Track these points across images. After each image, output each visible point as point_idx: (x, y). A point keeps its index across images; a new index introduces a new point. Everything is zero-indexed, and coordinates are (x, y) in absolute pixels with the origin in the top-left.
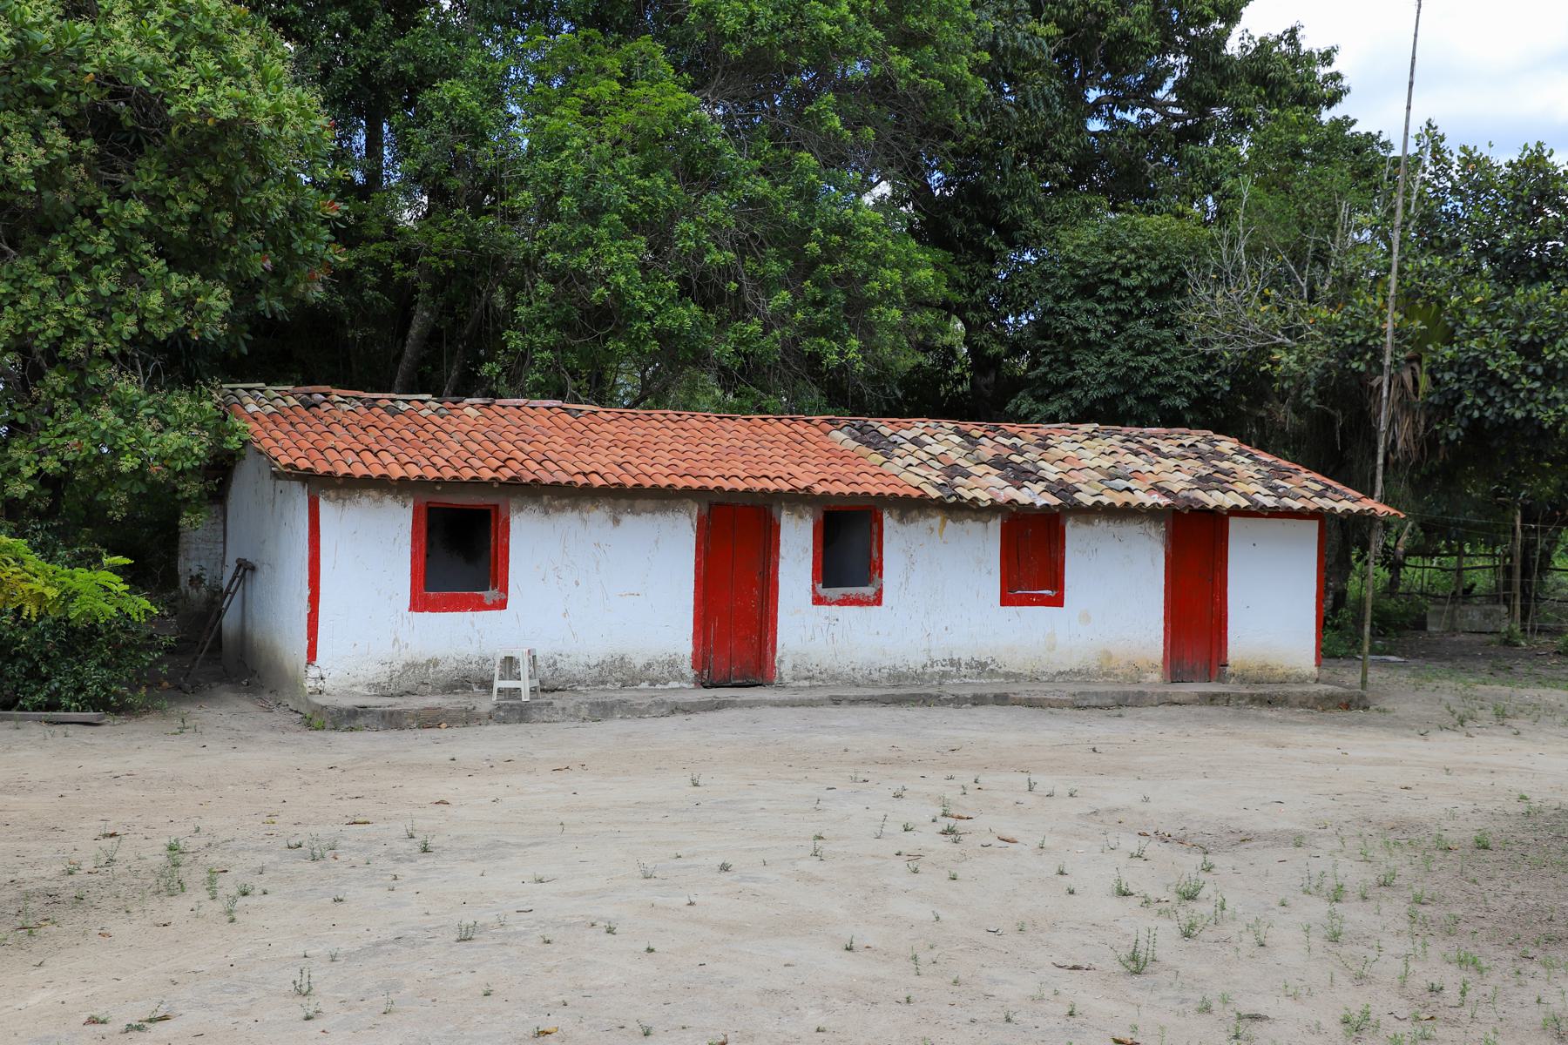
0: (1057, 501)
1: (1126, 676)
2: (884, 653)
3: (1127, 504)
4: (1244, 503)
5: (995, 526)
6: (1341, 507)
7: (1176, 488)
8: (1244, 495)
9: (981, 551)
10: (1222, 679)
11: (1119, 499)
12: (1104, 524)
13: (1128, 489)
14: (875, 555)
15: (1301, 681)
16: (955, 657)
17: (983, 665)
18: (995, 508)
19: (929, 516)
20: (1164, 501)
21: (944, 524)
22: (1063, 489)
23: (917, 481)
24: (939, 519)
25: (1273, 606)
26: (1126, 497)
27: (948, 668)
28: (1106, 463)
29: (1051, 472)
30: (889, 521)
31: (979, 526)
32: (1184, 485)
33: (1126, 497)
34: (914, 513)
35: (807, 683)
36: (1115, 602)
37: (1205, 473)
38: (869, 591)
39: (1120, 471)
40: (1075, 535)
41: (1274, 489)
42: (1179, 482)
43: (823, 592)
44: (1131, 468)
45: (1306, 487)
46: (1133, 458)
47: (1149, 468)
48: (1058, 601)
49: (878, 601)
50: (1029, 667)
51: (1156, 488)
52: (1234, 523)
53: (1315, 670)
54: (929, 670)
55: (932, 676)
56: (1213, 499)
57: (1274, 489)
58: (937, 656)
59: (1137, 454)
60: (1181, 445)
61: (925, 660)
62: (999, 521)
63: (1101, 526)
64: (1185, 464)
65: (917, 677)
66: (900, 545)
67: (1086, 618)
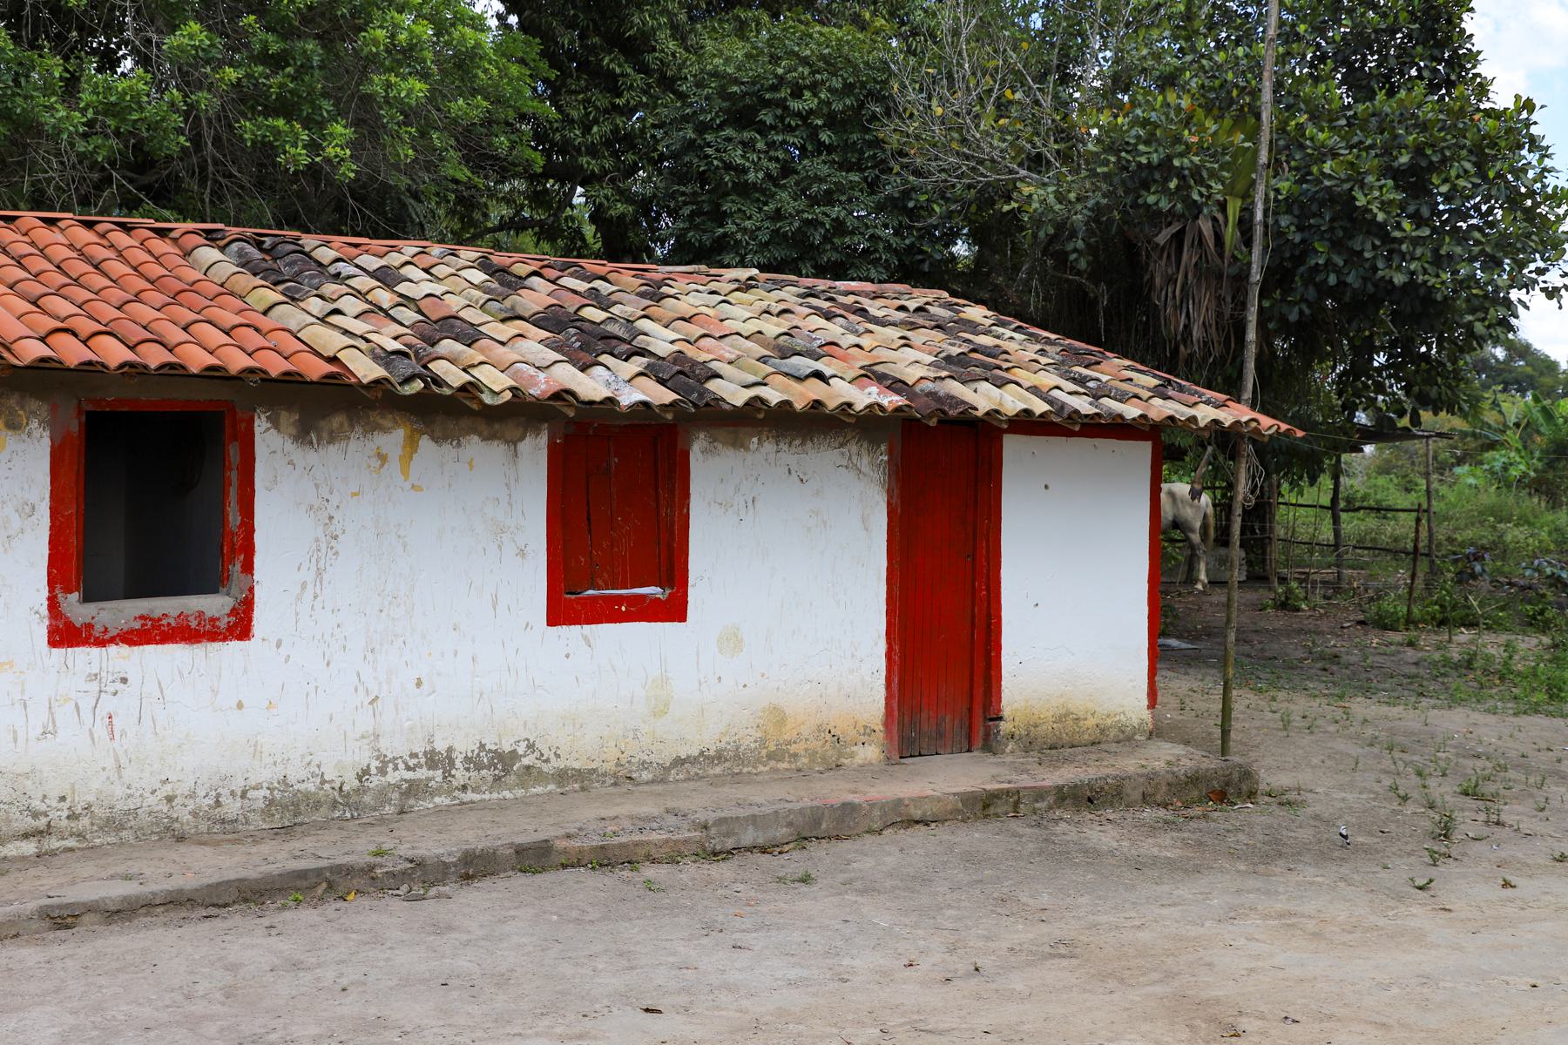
0: (668, 396)
1: (812, 755)
2: (257, 751)
3: (817, 403)
4: (1039, 407)
5: (534, 453)
6: (1205, 414)
7: (911, 375)
8: (1034, 390)
9: (499, 515)
10: (990, 745)
11: (802, 395)
12: (769, 446)
13: (818, 375)
14: (234, 518)
15: (1126, 738)
16: (441, 746)
17: (501, 763)
18: (521, 413)
19: (376, 427)
20: (891, 400)
21: (412, 445)
22: (682, 373)
23: (330, 341)
24: (399, 434)
25: (1075, 607)
26: (814, 390)
27: (423, 773)
28: (772, 327)
29: (661, 340)
30: (271, 445)
31: (497, 450)
32: (920, 372)
33: (814, 390)
34: (337, 420)
35: (29, 848)
36: (786, 605)
37: (955, 351)
38: (215, 605)
39: (799, 343)
40: (713, 476)
41: (1081, 381)
42: (914, 363)
43: (77, 609)
44: (823, 337)
45: (1133, 389)
46: (822, 322)
47: (852, 339)
48: (675, 610)
49: (240, 626)
50: (612, 754)
51: (871, 374)
52: (1012, 446)
53: (1146, 715)
54: (375, 781)
55: (382, 794)
56: (983, 398)
57: (1081, 381)
58: (395, 746)
59: (829, 317)
60: (902, 308)
61: (365, 758)
62: (543, 440)
63: (763, 452)
64: (918, 337)
65: (345, 805)
66: (294, 501)
67: (732, 641)
